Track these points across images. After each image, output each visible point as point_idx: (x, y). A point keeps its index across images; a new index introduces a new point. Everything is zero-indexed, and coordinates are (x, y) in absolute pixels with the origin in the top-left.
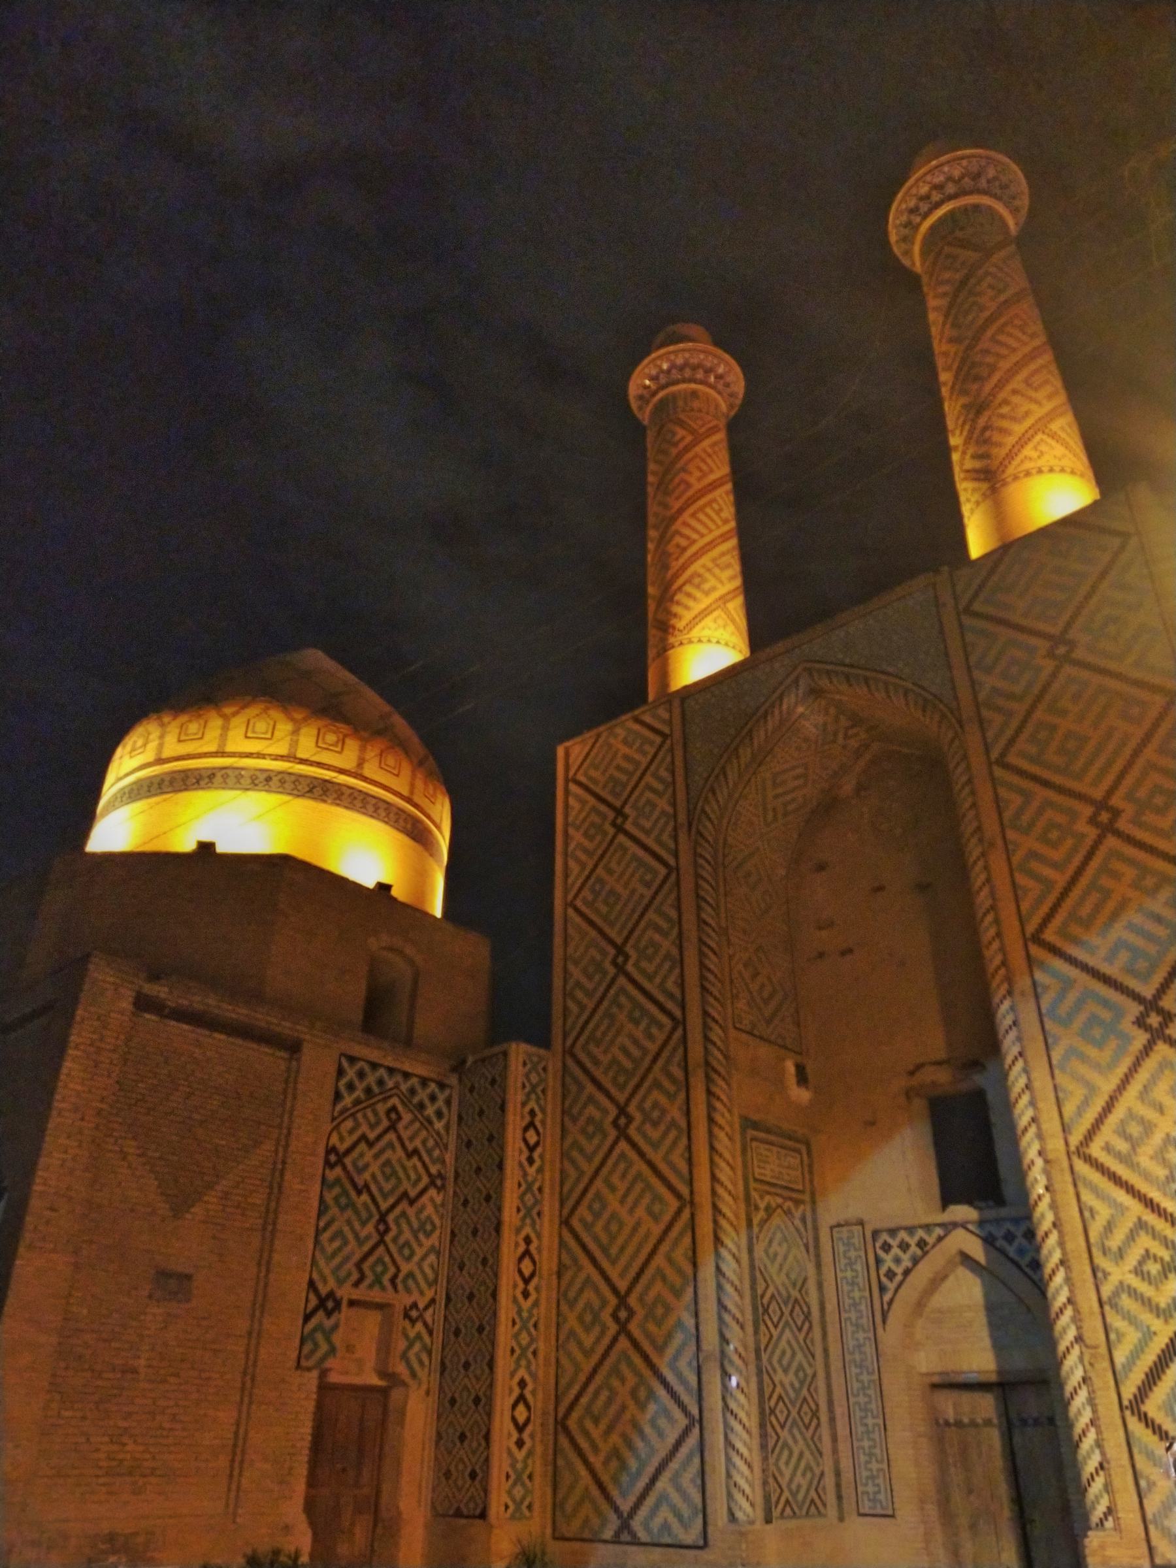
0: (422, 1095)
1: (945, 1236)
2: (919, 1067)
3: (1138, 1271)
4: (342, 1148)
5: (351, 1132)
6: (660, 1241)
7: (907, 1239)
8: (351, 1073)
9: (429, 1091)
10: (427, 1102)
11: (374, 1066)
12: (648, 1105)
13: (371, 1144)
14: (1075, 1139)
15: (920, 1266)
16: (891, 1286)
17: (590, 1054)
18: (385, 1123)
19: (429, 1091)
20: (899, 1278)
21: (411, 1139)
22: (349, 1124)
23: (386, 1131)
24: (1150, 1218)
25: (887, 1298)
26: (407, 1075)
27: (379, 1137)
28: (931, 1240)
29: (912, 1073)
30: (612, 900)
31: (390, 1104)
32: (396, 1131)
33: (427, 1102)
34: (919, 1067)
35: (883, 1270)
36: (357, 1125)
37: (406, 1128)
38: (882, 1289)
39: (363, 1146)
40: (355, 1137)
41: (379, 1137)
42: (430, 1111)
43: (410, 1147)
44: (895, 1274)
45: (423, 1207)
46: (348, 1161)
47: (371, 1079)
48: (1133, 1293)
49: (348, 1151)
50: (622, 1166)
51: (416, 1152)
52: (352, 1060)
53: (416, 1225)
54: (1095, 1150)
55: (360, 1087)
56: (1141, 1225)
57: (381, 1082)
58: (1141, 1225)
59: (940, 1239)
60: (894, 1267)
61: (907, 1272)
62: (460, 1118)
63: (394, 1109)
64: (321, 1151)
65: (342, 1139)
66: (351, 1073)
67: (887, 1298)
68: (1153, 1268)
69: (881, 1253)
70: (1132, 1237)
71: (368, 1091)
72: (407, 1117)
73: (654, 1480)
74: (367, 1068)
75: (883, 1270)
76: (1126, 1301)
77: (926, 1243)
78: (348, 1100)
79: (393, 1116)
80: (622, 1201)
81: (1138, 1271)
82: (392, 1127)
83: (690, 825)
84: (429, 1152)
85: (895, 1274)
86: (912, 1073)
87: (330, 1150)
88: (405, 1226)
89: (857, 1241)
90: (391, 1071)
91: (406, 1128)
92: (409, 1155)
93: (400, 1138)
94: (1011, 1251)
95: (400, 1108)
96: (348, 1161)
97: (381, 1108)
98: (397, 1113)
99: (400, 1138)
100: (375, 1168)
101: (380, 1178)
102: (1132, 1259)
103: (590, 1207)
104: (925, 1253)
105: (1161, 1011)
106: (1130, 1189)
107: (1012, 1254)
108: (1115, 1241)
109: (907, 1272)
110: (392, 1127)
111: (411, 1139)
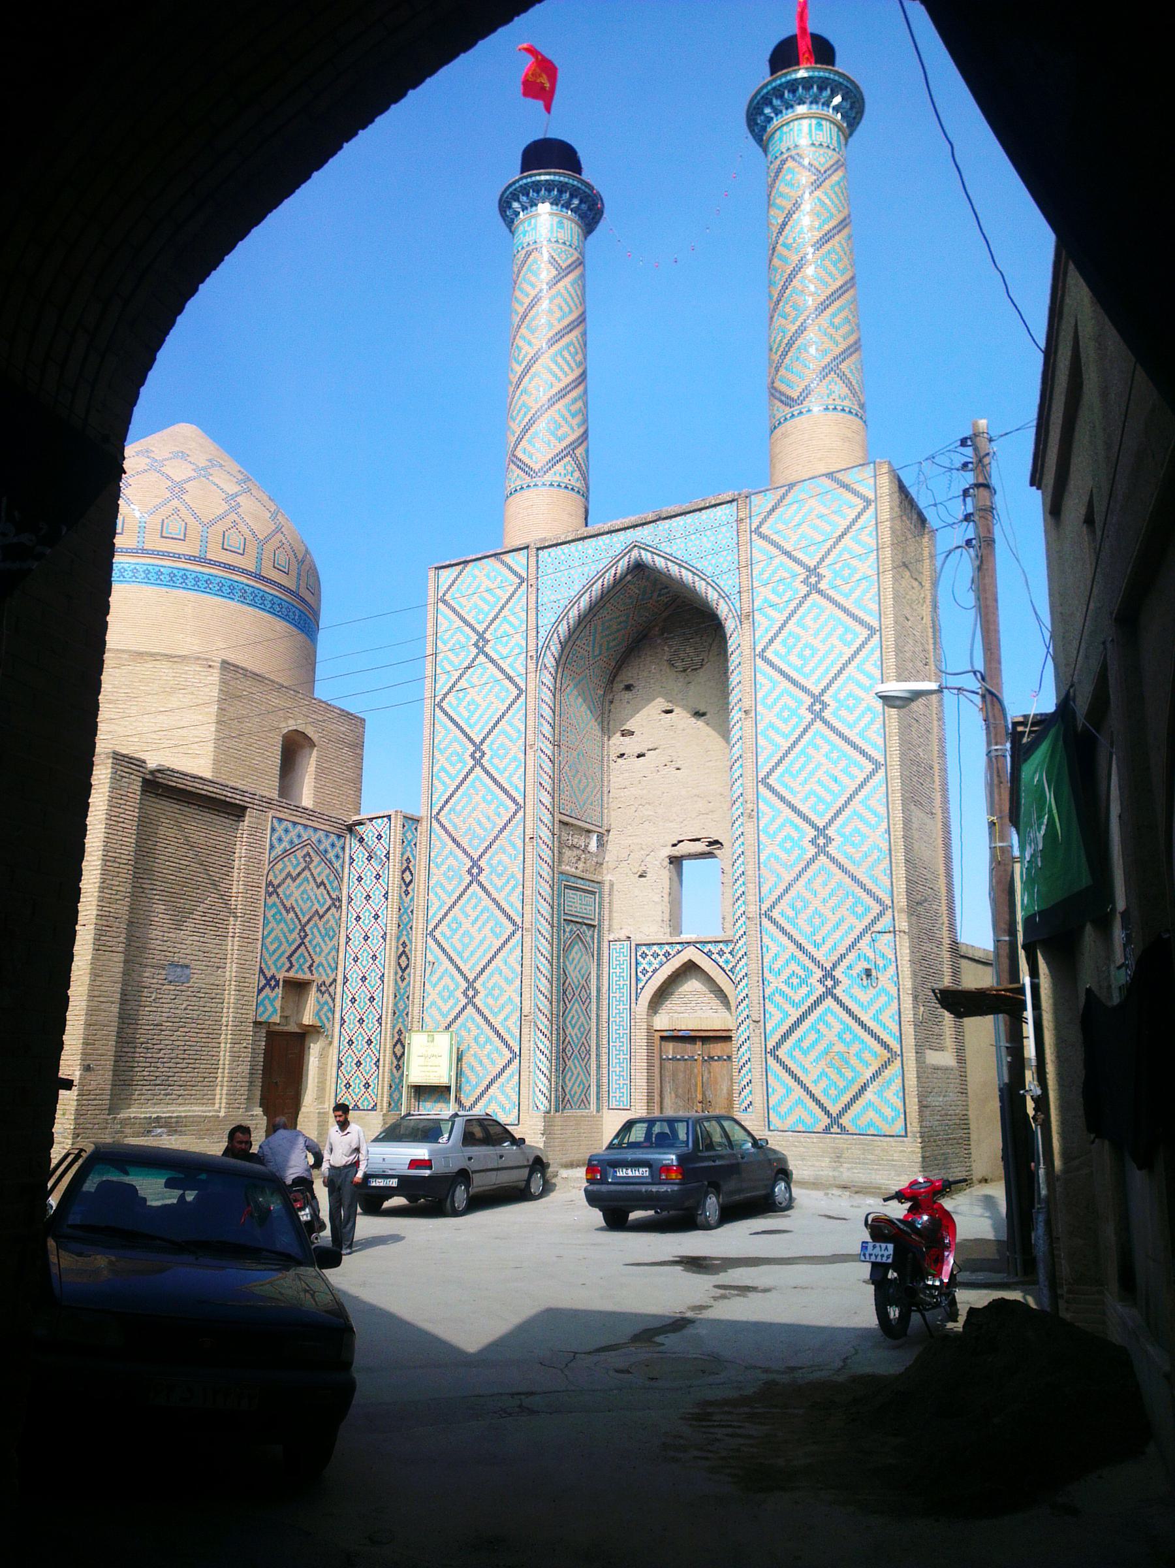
0: (326, 844)
3: (787, 982)
4: (276, 883)
5: (281, 871)
6: (499, 950)
7: (658, 951)
8: (280, 831)
9: (330, 840)
11: (295, 823)
12: (494, 862)
13: (294, 880)
14: (765, 907)
16: (645, 979)
17: (450, 821)
18: (304, 865)
19: (330, 840)
21: (319, 874)
22: (280, 866)
24: (799, 954)
25: (640, 986)
26: (316, 829)
27: (299, 874)
28: (672, 953)
29: (674, 845)
30: (472, 707)
31: (305, 852)
33: (329, 849)
36: (285, 866)
38: (637, 980)
39: (289, 880)
40: (283, 875)
41: (299, 874)
42: (331, 855)
43: (319, 881)
45: (328, 921)
46: (280, 890)
47: (293, 834)
48: (782, 994)
49: (279, 886)
50: (474, 901)
51: (322, 883)
52: (280, 820)
53: (323, 931)
54: (775, 914)
55: (286, 839)
56: (793, 957)
57: (299, 836)
58: (793, 957)
59: (679, 952)
60: (647, 968)
61: (655, 971)
63: (308, 854)
64: (264, 885)
65: (276, 877)
66: (280, 831)
67: (640, 986)
68: (795, 981)
70: (787, 962)
71: (291, 842)
72: (317, 859)
73: (488, 1087)
74: (290, 825)
76: (777, 998)
78: (279, 850)
79: (308, 859)
80: (473, 923)
81: (787, 982)
82: (307, 868)
83: (538, 658)
84: (331, 883)
86: (674, 845)
87: (270, 884)
88: (317, 934)
89: (626, 950)
90: (306, 826)
91: (316, 867)
92: (318, 887)
93: (312, 874)
94: (721, 961)
95: (312, 854)
96: (280, 890)
97: (300, 854)
99: (312, 874)
100: (297, 894)
101: (300, 901)
102: (784, 976)
103: (449, 926)
105: (826, 837)
106: (791, 938)
108: (777, 966)
110: (307, 868)
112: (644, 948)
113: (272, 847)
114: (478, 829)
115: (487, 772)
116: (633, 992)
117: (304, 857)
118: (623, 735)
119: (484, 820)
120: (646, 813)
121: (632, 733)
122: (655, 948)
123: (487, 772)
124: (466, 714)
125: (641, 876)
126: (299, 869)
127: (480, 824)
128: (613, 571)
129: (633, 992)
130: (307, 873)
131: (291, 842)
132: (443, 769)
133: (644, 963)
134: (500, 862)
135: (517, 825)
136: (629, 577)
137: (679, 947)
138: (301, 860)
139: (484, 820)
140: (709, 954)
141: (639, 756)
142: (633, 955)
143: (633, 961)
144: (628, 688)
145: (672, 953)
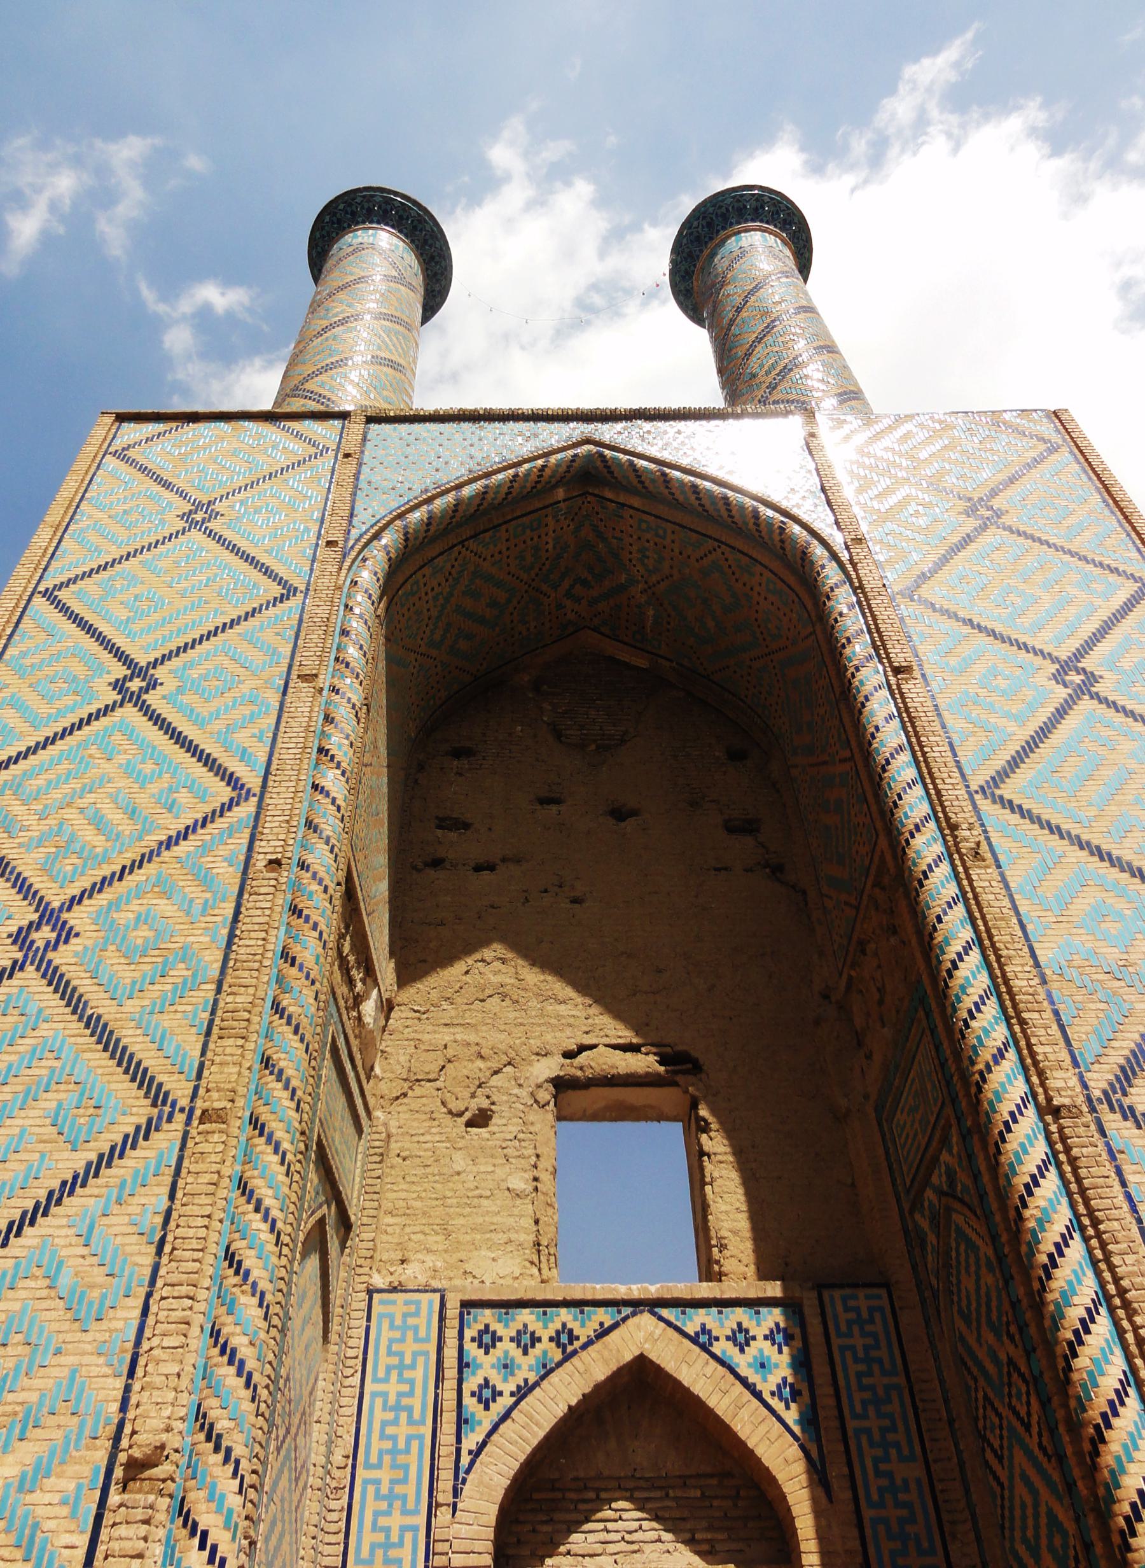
1: (615, 1326)
2: (583, 1048)
6: (70, 1187)
14: (1098, 1081)
15: (554, 1378)
16: (486, 1419)
20: (506, 1401)
25: (470, 1441)
28: (584, 1332)
29: (569, 1055)
34: (583, 1048)
35: (472, 1383)
38: (461, 1421)
44: (497, 1394)
59: (604, 1332)
60: (496, 1379)
61: (522, 1393)
67: (470, 1441)
69: (471, 1349)
75: (472, 1383)
77: (572, 1337)
85: (497, 1394)
89: (426, 1323)
94: (743, 1363)
104: (567, 1357)
107: (743, 1371)
109: (522, 1393)
112: (487, 1316)
114: (89, 835)
115: (157, 720)
116: (446, 1464)
118: (439, 827)
119: (114, 816)
120: (495, 979)
121: (467, 826)
122: (526, 1316)
123: (157, 720)
125: (470, 1124)
127: (98, 823)
128: (540, 462)
129: (446, 1464)
133: (485, 1366)
134: (141, 920)
135: (231, 831)
136: (560, 494)
137: (605, 1316)
139: (114, 816)
140: (702, 1341)
141: (478, 869)
142: (451, 1334)
143: (450, 1353)
144: (458, 753)
145: (584, 1332)
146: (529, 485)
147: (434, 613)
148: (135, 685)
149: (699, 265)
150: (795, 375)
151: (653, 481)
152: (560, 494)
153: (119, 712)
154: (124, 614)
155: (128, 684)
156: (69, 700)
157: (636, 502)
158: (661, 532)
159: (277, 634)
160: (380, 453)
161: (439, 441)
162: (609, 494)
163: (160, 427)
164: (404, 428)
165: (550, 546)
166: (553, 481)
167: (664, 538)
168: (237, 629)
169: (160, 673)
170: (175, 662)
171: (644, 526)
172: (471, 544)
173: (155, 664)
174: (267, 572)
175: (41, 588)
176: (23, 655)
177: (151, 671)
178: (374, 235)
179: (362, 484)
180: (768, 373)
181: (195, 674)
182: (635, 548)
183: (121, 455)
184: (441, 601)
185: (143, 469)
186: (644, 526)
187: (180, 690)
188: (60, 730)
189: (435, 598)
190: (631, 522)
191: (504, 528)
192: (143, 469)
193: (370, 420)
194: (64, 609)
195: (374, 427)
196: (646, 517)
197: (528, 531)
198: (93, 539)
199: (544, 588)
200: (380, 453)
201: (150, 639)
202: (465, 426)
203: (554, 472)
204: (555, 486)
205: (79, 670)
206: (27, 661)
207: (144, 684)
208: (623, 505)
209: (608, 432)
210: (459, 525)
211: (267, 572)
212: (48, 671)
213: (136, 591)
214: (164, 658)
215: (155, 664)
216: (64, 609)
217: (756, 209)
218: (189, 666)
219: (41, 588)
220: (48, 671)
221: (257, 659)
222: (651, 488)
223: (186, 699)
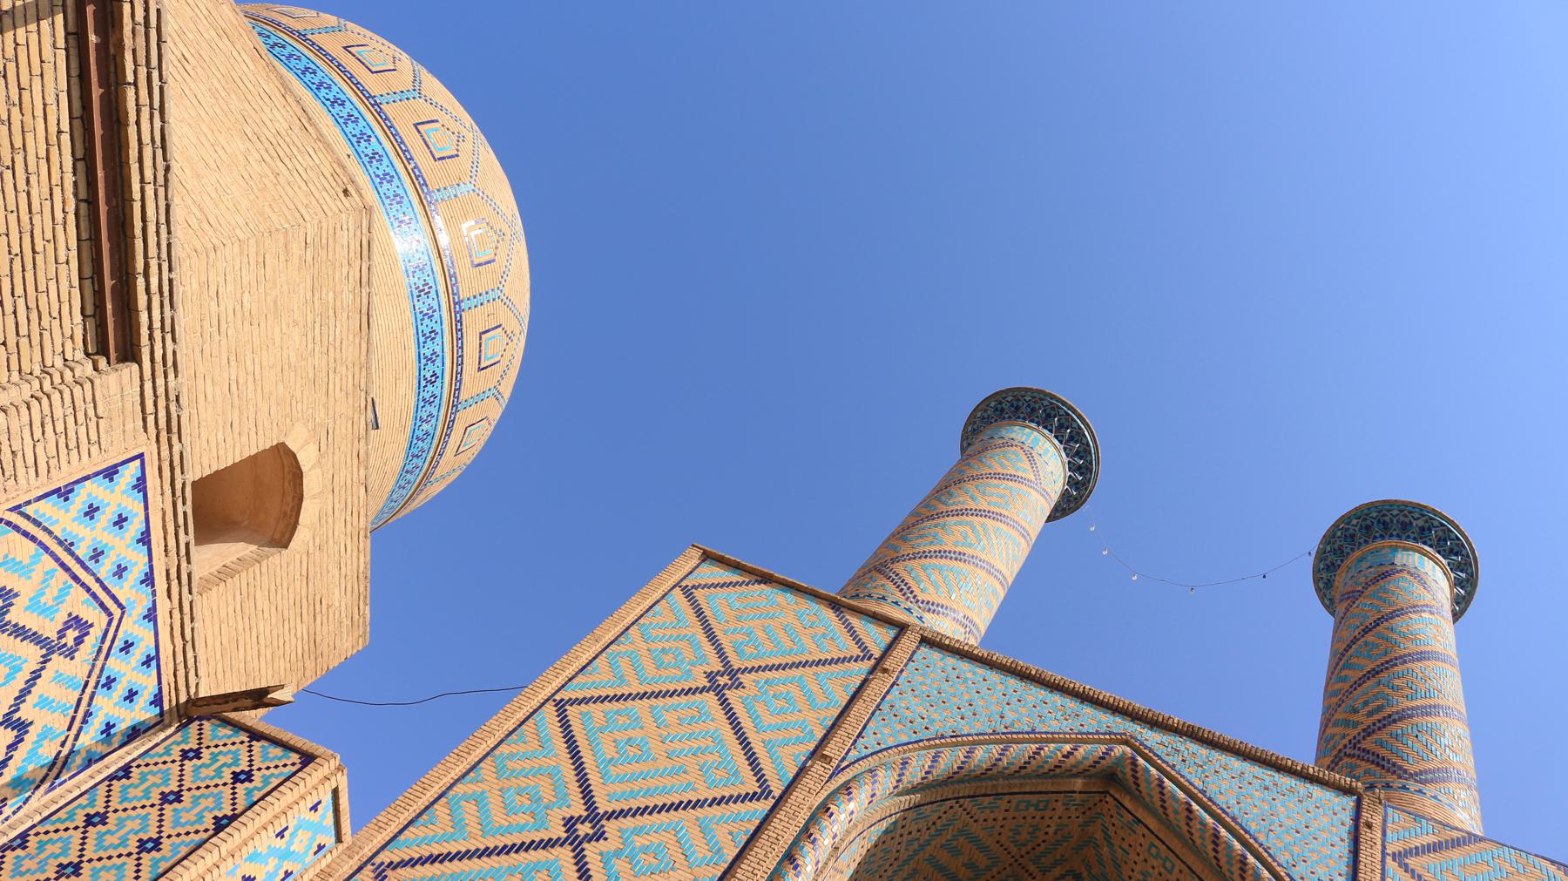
0: (126, 670)
10: (120, 690)
11: (145, 539)
21: (44, 703)
23: (36, 639)
30: (632, 751)
31: (92, 614)
32: (46, 660)
33: (120, 690)
36: (24, 570)
37: (58, 678)
43: (24, 713)
51: (22, 727)
52: (141, 485)
62: (126, 771)
74: (135, 527)
79: (71, 635)
82: (50, 648)
93: (36, 675)
98: (79, 641)
99: (36, 675)
110: (50, 648)
111: (44, 703)
113: (64, 493)
117: (75, 622)
124: (608, 751)
126: (32, 622)
130: (32, 653)
131: (97, 555)
132: (478, 800)
136: (1078, 784)
138: (62, 617)
146: (1047, 767)
147: (903, 856)
148: (584, 829)
149: (1347, 562)
150: (1397, 728)
151: (1176, 812)
152: (1078, 784)
153: (557, 850)
154: (608, 751)
155: (578, 826)
156: (522, 819)
157: (1152, 823)
158: (1168, 865)
159: (731, 833)
160: (917, 678)
161: (978, 686)
162: (1127, 803)
163: (736, 578)
164: (951, 661)
165: (1051, 831)
166: (1075, 771)
167: (1170, 872)
168: (699, 812)
169: (610, 827)
170: (628, 822)
171: (1154, 850)
172: (967, 803)
173: (610, 816)
174: (753, 760)
175: (558, 697)
176: (512, 755)
177: (604, 822)
178: (1028, 436)
179: (885, 706)
180: (1370, 714)
181: (639, 841)
182: (1137, 868)
183: (688, 593)
184: (916, 846)
185: (699, 613)
186: (1154, 850)
187: (618, 854)
188: (501, 845)
189: (909, 843)
190: (1142, 840)
191: (1007, 798)
192: (699, 613)
193: (924, 641)
194: (565, 725)
195: (924, 650)
196: (1157, 843)
197: (1032, 809)
198: (624, 667)
199: (1032, 868)
200: (917, 678)
201: (618, 788)
202: (1013, 682)
203: (1079, 763)
204: (1077, 775)
205: (546, 792)
206: (510, 765)
207: (591, 832)
208: (1140, 821)
209: (1152, 738)
210: (961, 781)
211: (753, 760)
212: (523, 782)
213: (630, 733)
214: (622, 813)
215: (610, 816)
216: (565, 725)
217: (1422, 529)
218: (638, 832)
219: (558, 697)
220: (523, 782)
221: (700, 852)
222: (1172, 816)
223: (619, 865)
